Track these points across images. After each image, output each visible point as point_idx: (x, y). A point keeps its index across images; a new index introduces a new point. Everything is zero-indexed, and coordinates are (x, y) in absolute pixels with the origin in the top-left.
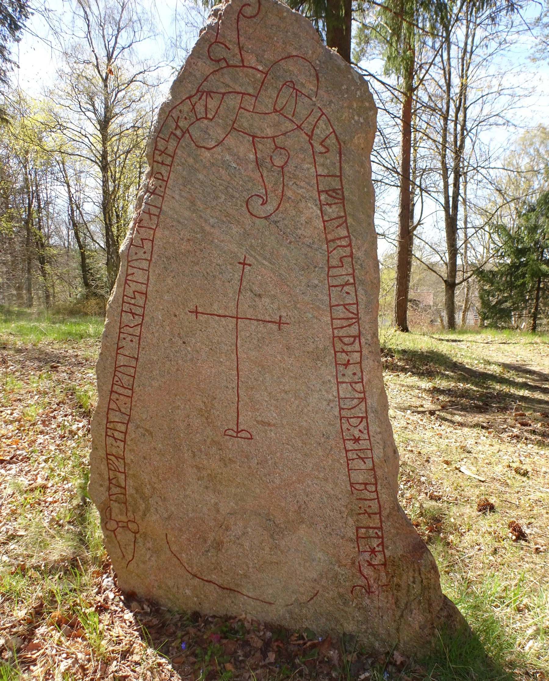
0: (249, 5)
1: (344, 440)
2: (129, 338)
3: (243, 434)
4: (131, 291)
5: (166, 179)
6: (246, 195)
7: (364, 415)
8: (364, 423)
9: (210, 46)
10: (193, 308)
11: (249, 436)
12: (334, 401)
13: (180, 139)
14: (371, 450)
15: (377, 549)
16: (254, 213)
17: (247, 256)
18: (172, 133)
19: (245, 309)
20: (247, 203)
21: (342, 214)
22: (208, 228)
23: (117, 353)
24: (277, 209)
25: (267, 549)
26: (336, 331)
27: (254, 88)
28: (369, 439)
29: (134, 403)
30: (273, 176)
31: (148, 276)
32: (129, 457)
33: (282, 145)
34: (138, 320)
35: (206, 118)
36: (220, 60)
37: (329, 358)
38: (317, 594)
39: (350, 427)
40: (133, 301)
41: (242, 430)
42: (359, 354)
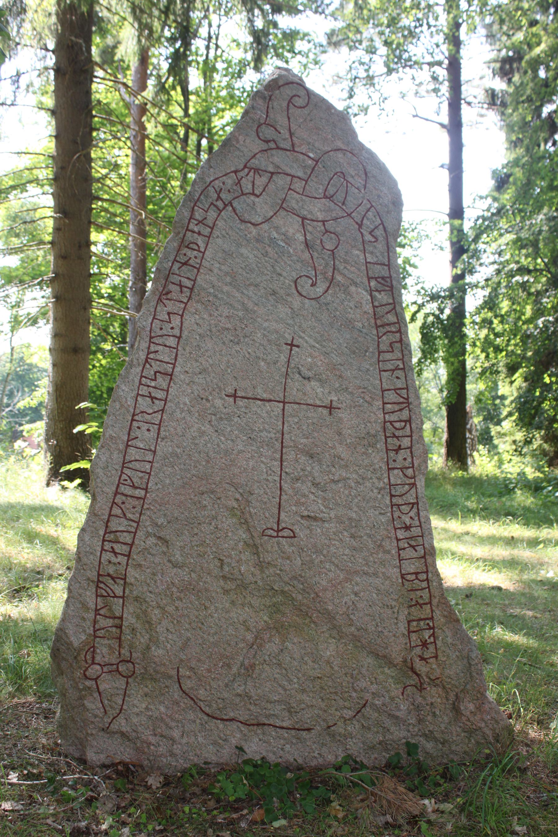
0: (299, 96)
1: (395, 529)
2: (145, 427)
3: (286, 533)
4: (153, 373)
5: (203, 250)
6: (295, 275)
7: (415, 501)
8: (415, 510)
9: (259, 127)
10: (231, 391)
11: (292, 535)
12: (384, 488)
13: (221, 211)
14: (422, 536)
15: (429, 641)
16: (304, 293)
17: (295, 337)
18: (212, 204)
19: (293, 393)
20: (295, 282)
21: (391, 301)
22: (250, 305)
23: (128, 446)
24: (326, 291)
25: (310, 662)
26: (387, 416)
27: (305, 173)
28: (421, 526)
29: (146, 506)
30: (323, 259)
31: (177, 355)
32: (133, 574)
33: (332, 230)
34: (159, 405)
35: (253, 194)
36: (269, 141)
37: (381, 445)
38: (365, 705)
39: (401, 515)
40: (153, 384)
41: (284, 528)
42: (409, 439)
